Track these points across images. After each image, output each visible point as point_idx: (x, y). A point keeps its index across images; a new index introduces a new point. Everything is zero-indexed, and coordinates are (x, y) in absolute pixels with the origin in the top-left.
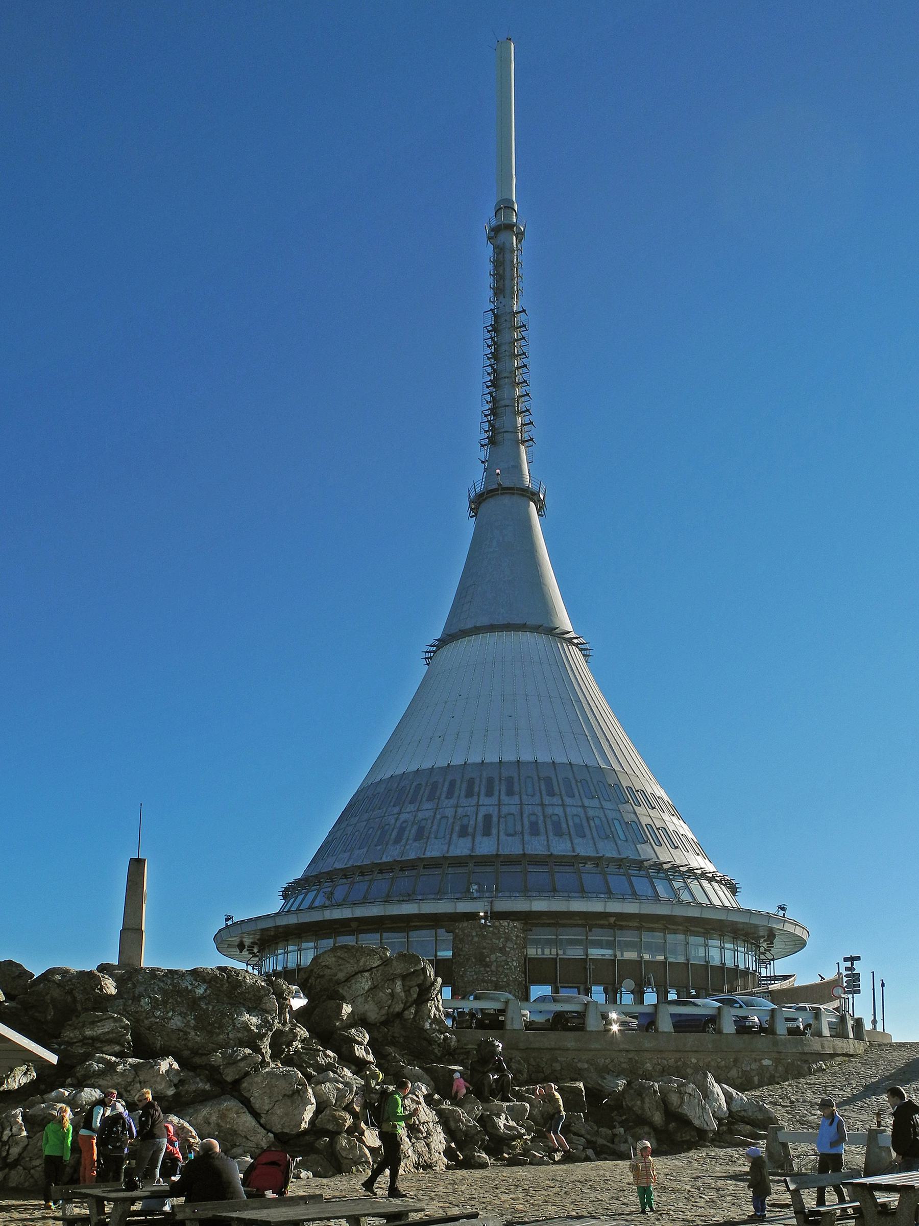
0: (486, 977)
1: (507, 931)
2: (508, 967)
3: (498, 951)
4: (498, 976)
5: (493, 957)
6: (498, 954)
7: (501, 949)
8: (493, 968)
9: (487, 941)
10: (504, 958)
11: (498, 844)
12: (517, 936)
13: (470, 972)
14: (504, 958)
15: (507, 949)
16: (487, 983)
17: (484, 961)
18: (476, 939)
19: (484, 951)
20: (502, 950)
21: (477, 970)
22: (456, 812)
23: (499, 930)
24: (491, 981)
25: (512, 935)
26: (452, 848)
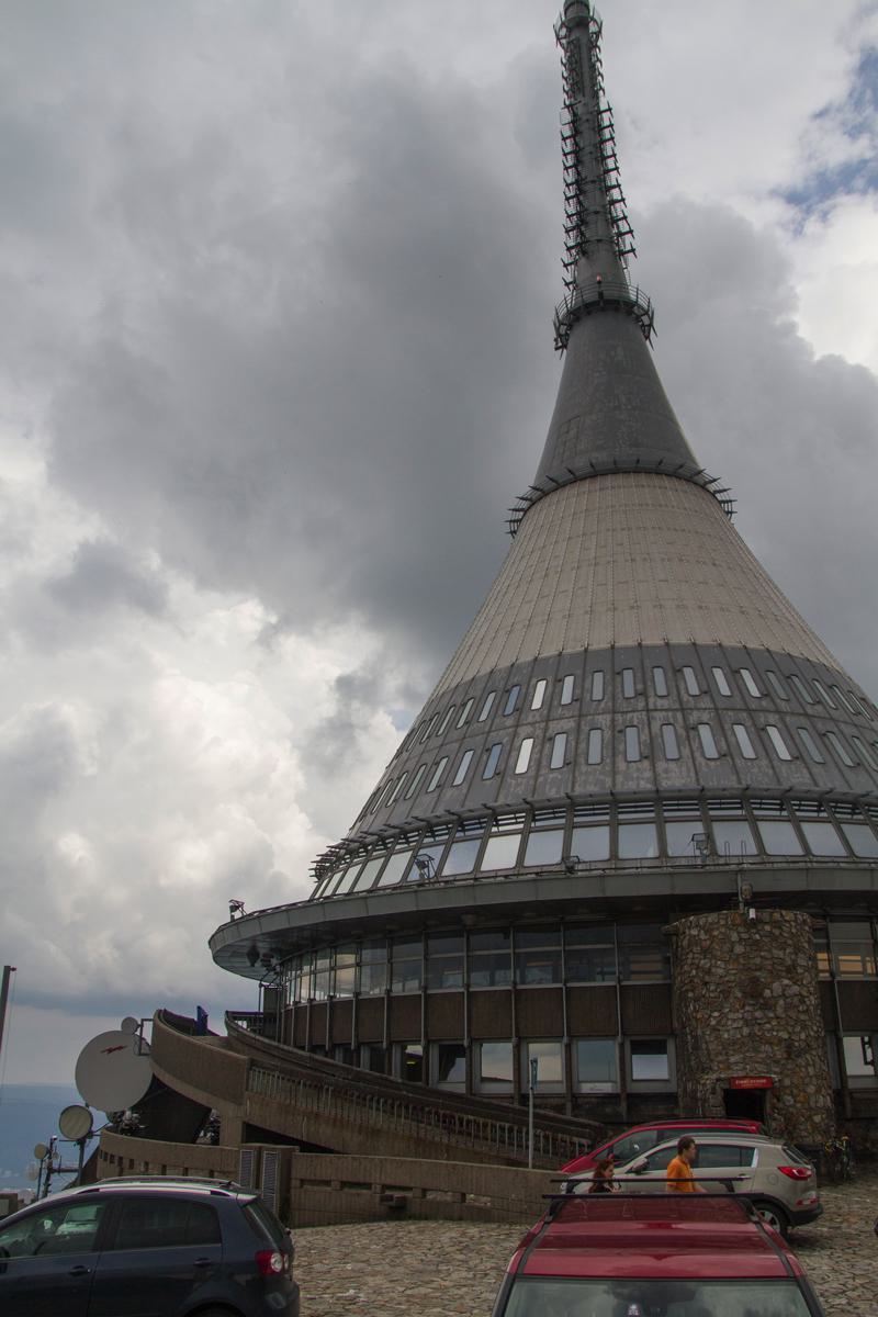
0: (769, 1031)
1: (794, 931)
3: (784, 974)
6: (786, 982)
7: (788, 970)
8: (780, 1011)
9: (762, 954)
10: (796, 989)
13: (734, 1020)
14: (796, 989)
15: (800, 971)
16: (771, 1044)
17: (761, 995)
18: (739, 949)
19: (758, 974)
22: (613, 720)
23: (780, 928)
24: (780, 1040)
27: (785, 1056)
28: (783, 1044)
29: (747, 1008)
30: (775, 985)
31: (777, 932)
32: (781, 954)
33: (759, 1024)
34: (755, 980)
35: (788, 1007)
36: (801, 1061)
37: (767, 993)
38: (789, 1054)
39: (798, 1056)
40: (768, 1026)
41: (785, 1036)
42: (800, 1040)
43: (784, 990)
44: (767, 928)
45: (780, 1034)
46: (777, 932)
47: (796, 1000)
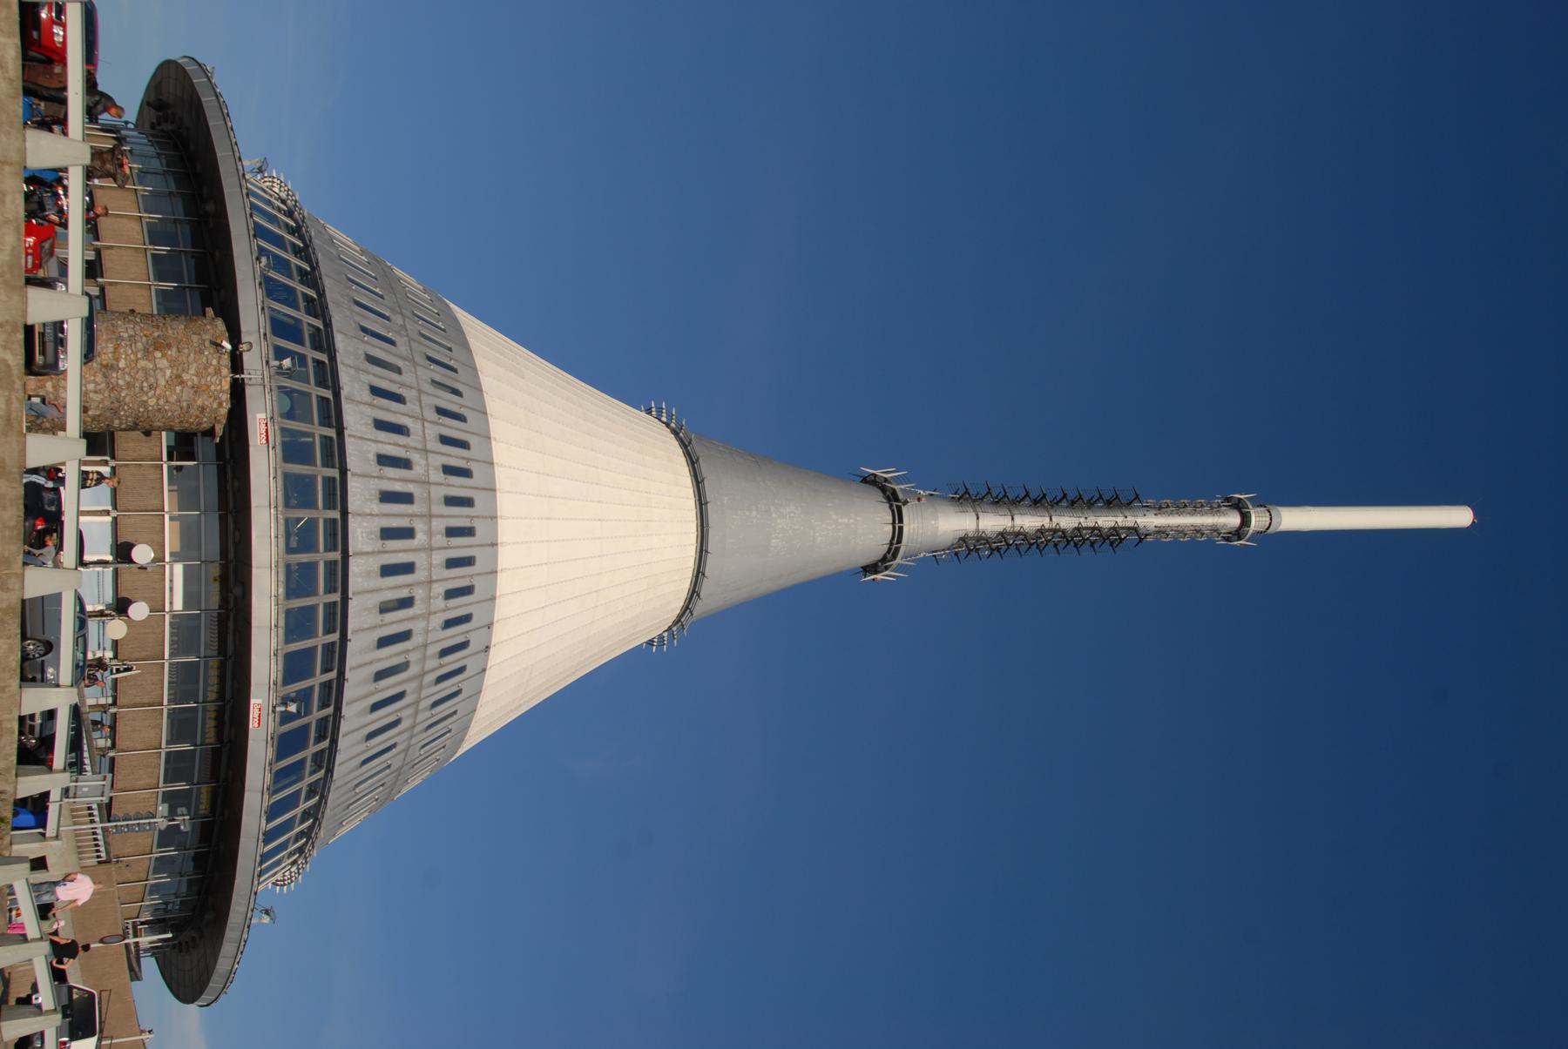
2: (145, 389)
4: (127, 370)
5: (163, 363)
6: (168, 372)
8: (142, 363)
10: (162, 382)
11: (361, 438)
12: (203, 409)
14: (162, 382)
15: (178, 389)
17: (156, 349)
19: (174, 349)
20: (178, 379)
21: (137, 338)
24: (117, 360)
25: (205, 397)
26: (352, 371)
27: (104, 362)
28: (114, 362)
29: (144, 338)
30: (165, 361)
31: (211, 370)
32: (192, 371)
33: (131, 345)
34: (169, 346)
35: (145, 370)
36: (99, 378)
37: (158, 354)
38: (106, 366)
39: (105, 376)
40: (130, 352)
41: (122, 364)
42: (118, 379)
43: (161, 369)
44: (215, 362)
45: (123, 361)
46: (211, 370)
47: (152, 380)
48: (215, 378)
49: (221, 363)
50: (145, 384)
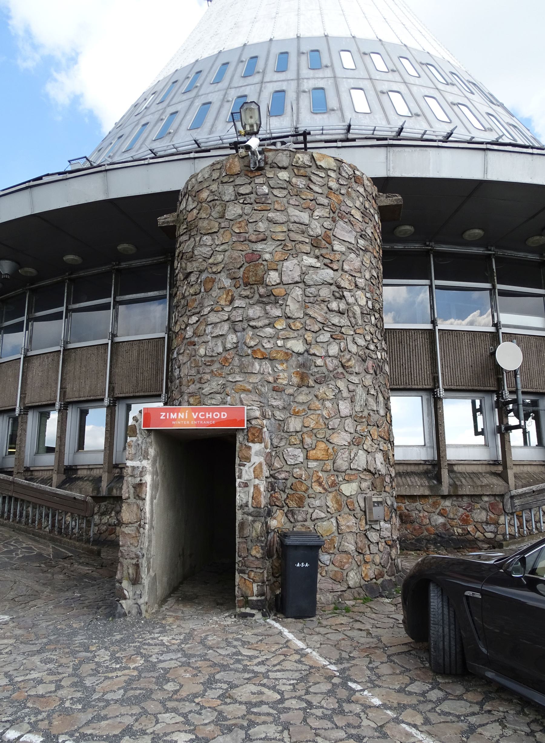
1: (333, 184)
3: (307, 248)
6: (310, 261)
27: (296, 380)
30: (286, 264)
31: (301, 182)
40: (269, 331)
41: (298, 346)
44: (284, 175)
45: (290, 344)
48: (314, 178)
49: (285, 163)
50: (334, 305)
